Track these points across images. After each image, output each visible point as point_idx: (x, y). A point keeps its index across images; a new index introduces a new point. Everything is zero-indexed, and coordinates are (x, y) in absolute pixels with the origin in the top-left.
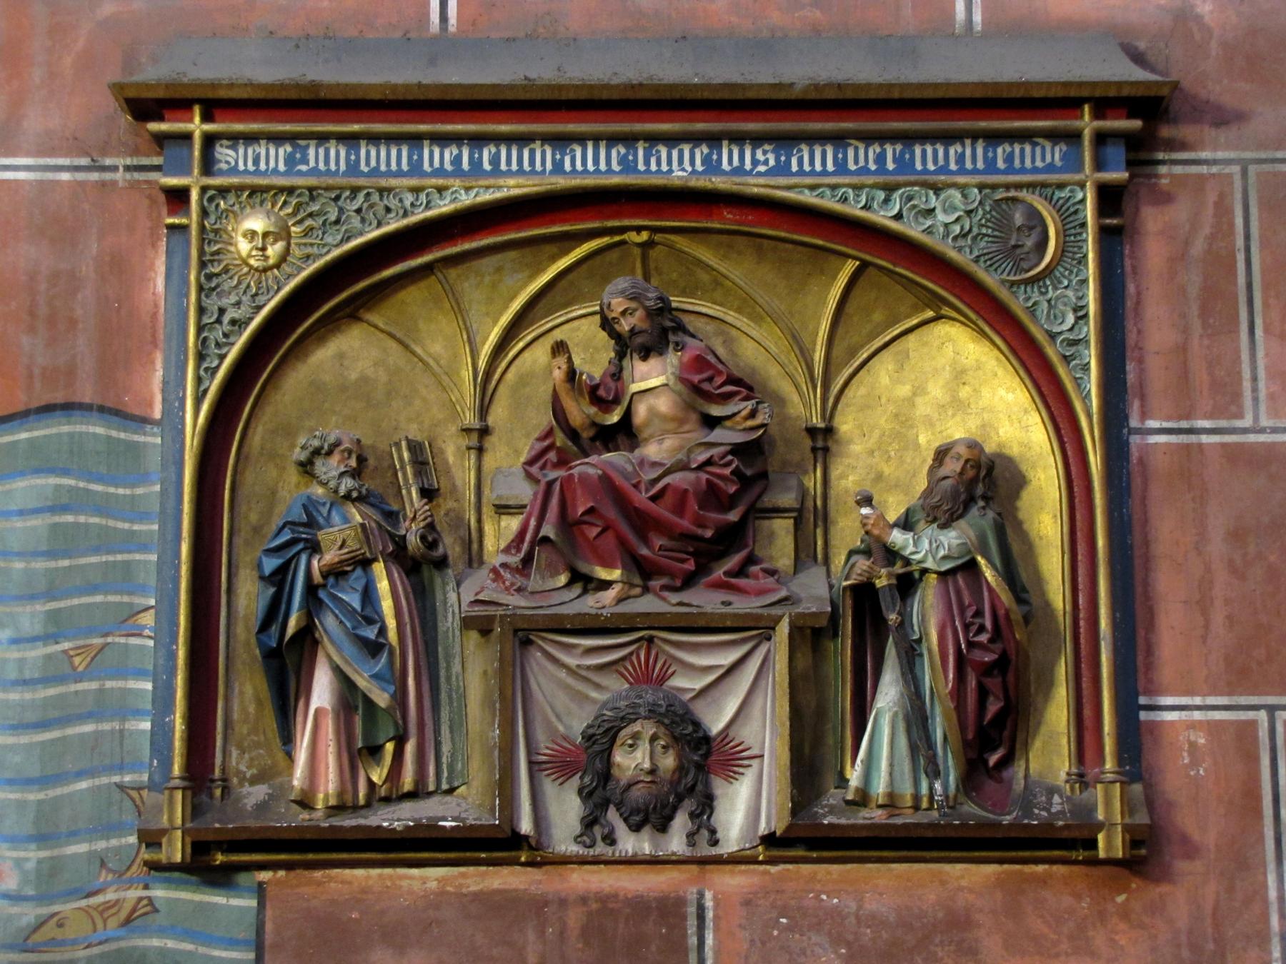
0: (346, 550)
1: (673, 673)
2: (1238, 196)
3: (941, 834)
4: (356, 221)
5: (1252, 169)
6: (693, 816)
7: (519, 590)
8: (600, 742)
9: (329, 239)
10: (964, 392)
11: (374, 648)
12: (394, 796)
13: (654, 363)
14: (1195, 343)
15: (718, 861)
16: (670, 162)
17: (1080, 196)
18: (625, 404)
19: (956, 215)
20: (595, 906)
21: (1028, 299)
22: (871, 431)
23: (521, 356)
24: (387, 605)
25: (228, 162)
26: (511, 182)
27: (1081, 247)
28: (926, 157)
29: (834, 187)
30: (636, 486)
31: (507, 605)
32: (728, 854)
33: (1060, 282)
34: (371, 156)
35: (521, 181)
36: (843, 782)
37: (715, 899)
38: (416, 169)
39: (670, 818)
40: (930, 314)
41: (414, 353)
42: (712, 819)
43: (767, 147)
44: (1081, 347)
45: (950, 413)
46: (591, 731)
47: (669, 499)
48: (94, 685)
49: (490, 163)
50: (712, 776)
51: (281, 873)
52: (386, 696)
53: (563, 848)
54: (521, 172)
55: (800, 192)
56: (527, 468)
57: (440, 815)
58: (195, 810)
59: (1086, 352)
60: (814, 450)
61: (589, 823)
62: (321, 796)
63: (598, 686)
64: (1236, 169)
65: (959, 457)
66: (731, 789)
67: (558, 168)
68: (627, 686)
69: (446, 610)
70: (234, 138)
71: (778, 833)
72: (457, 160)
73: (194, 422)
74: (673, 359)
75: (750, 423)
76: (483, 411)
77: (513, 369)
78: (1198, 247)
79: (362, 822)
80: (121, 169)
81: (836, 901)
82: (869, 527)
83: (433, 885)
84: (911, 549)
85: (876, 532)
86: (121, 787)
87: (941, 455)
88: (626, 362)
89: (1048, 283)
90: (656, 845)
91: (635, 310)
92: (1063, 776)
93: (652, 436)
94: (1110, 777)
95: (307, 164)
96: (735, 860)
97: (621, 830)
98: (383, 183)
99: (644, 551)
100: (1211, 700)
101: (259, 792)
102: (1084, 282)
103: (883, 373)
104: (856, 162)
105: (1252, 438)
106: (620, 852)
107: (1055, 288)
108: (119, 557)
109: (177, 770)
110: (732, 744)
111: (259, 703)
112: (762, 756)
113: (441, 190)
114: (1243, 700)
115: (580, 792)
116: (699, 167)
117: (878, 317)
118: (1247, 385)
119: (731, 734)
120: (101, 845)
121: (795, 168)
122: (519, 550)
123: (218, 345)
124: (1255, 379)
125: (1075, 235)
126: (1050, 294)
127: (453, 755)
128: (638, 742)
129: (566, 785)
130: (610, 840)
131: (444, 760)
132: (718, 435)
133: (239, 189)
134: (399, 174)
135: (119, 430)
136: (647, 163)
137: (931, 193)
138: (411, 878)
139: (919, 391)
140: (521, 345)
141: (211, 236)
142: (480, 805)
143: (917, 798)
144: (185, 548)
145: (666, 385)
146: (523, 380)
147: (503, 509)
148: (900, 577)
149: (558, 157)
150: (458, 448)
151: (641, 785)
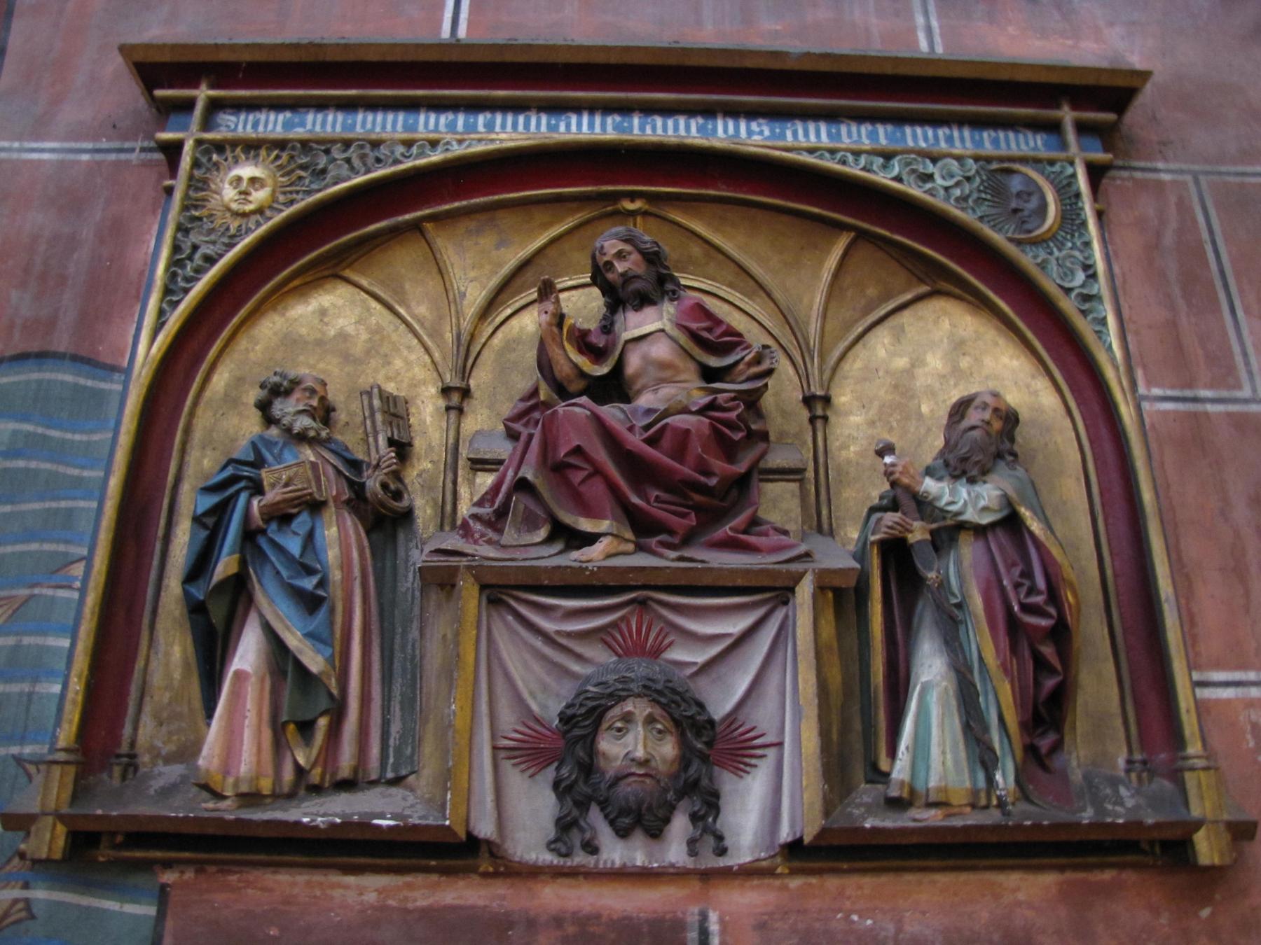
0: (290, 488)
1: (671, 644)
2: (1195, 199)
3: (1007, 838)
4: (345, 170)
5: (1202, 178)
6: (695, 818)
7: (490, 542)
8: (582, 724)
10: (965, 363)
11: (310, 603)
12: (327, 785)
13: (649, 311)
14: (1183, 321)
15: (727, 874)
17: (1070, 171)
18: (617, 353)
20: (571, 929)
22: (871, 402)
23: (509, 322)
27: (1079, 215)
28: (917, 137)
30: (631, 429)
31: (473, 556)
33: (1063, 244)
36: (879, 776)
37: (721, 921)
39: (667, 821)
40: (924, 289)
42: (719, 822)
44: (1094, 304)
45: (952, 383)
46: (570, 712)
47: (666, 442)
50: (716, 768)
51: (189, 875)
52: (320, 659)
53: (533, 856)
55: (800, 154)
56: (510, 424)
57: (378, 810)
58: (80, 792)
59: (1101, 307)
60: (812, 420)
61: (565, 826)
63: (579, 658)
65: (985, 406)
66: (741, 784)
68: (615, 658)
69: (407, 568)
71: (807, 840)
72: (452, 127)
74: (669, 308)
75: (755, 370)
76: (465, 372)
77: (500, 334)
78: (1169, 239)
79: (278, 815)
80: (138, 150)
81: (869, 922)
82: (897, 475)
83: (371, 897)
84: (946, 498)
85: (905, 480)
86: (19, 760)
87: (960, 409)
88: (619, 317)
89: (1051, 244)
90: (650, 855)
91: (630, 253)
92: (1121, 762)
93: (644, 388)
96: (749, 872)
97: (605, 836)
99: (635, 500)
102: (1087, 244)
103: (879, 346)
106: (605, 862)
107: (1060, 250)
108: (63, 504)
110: (741, 730)
111: (186, 664)
112: (780, 745)
113: (434, 144)
115: (556, 785)
117: (872, 292)
118: (1239, 359)
119: (741, 718)
122: (493, 503)
124: (1245, 354)
126: (1056, 253)
127: (403, 737)
128: (629, 726)
129: (538, 777)
130: (591, 848)
131: (391, 742)
135: (87, 377)
138: (347, 887)
139: (917, 362)
140: (509, 311)
141: (200, 185)
142: (430, 800)
143: (975, 793)
145: (662, 331)
146: (509, 346)
147: (479, 464)
148: (932, 533)
150: (437, 409)
151: (632, 779)
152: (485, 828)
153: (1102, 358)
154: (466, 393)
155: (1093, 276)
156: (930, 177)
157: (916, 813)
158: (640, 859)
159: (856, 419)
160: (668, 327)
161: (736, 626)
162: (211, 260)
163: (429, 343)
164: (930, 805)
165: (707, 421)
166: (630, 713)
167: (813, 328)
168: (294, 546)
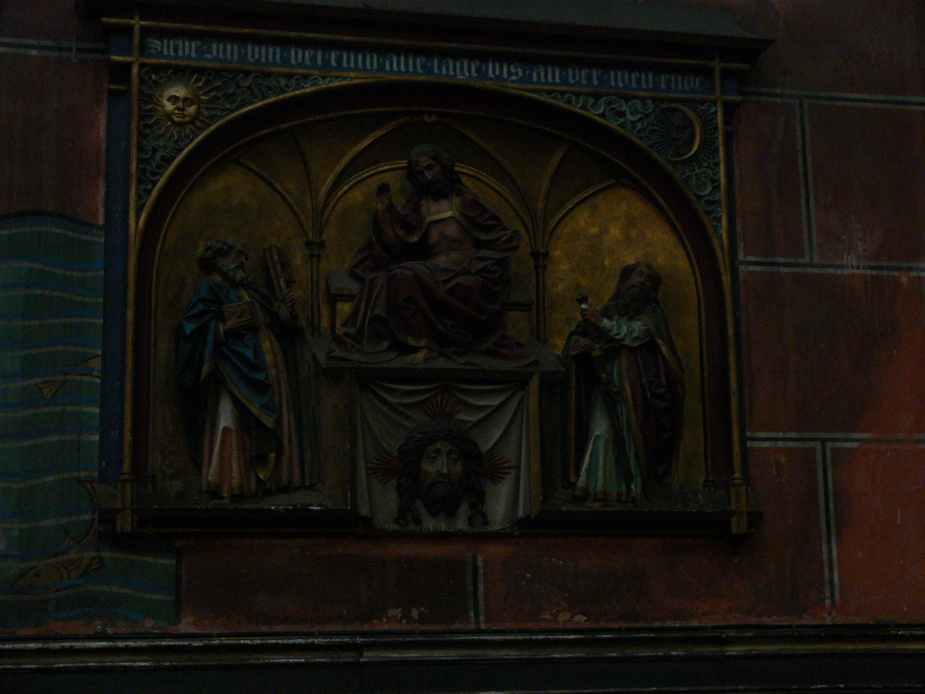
0: (244, 319)
5: (806, 101)
6: (472, 506)
7: (358, 351)
9: (228, 106)
10: (634, 234)
11: (261, 388)
13: (444, 204)
16: (455, 70)
17: (713, 109)
18: (423, 230)
19: (639, 116)
21: (684, 173)
24: (268, 358)
25: (156, 49)
26: (352, 74)
27: (714, 143)
28: (618, 79)
29: (563, 93)
31: (353, 361)
32: (495, 531)
33: (702, 164)
34: (254, 53)
35: (359, 74)
37: (484, 561)
38: (286, 61)
40: (613, 181)
41: (275, 189)
43: (517, 64)
45: (625, 247)
48: (58, 409)
49: (336, 62)
54: (356, 69)
55: (542, 95)
59: (719, 209)
60: (537, 267)
61: (403, 510)
62: (225, 488)
63: (408, 417)
64: (797, 101)
65: (642, 273)
67: (381, 67)
70: (162, 34)
71: (532, 516)
72: (313, 59)
73: (136, 223)
74: (456, 200)
75: (506, 246)
77: (340, 204)
80: (74, 50)
81: (561, 562)
82: (588, 317)
84: (615, 331)
85: (593, 320)
86: (79, 480)
89: (694, 164)
92: (701, 481)
94: (738, 482)
95: (212, 54)
96: (499, 536)
98: (265, 69)
99: (440, 327)
100: (788, 435)
101: (176, 486)
104: (574, 78)
105: (809, 270)
107: (699, 168)
108: (75, 320)
109: (126, 466)
110: (496, 459)
112: (518, 467)
113: (306, 77)
114: (807, 435)
115: (398, 489)
116: (474, 75)
118: (805, 236)
120: (64, 520)
121: (535, 79)
123: (154, 174)
124: (810, 233)
125: (711, 134)
126: (697, 171)
130: (418, 521)
132: (483, 253)
133: (168, 67)
134: (275, 64)
136: (440, 69)
137: (623, 101)
143: (619, 494)
144: (130, 314)
145: (451, 217)
149: (381, 60)
152: (364, 511)
153: (716, 243)
154: (321, 244)
155: (717, 188)
156: (622, 114)
157: (588, 504)
158: (443, 527)
159: (564, 267)
160: (456, 216)
161: (496, 401)
162: (168, 160)
163: (297, 209)
164: (596, 500)
165: (481, 279)
166: (439, 449)
167: (540, 205)
168: (249, 354)
